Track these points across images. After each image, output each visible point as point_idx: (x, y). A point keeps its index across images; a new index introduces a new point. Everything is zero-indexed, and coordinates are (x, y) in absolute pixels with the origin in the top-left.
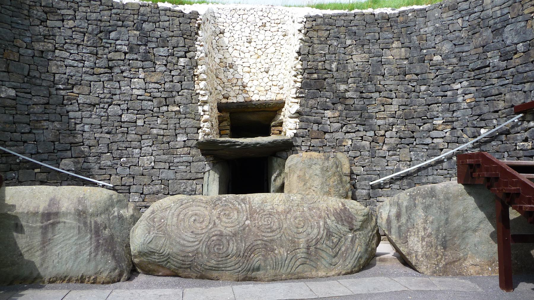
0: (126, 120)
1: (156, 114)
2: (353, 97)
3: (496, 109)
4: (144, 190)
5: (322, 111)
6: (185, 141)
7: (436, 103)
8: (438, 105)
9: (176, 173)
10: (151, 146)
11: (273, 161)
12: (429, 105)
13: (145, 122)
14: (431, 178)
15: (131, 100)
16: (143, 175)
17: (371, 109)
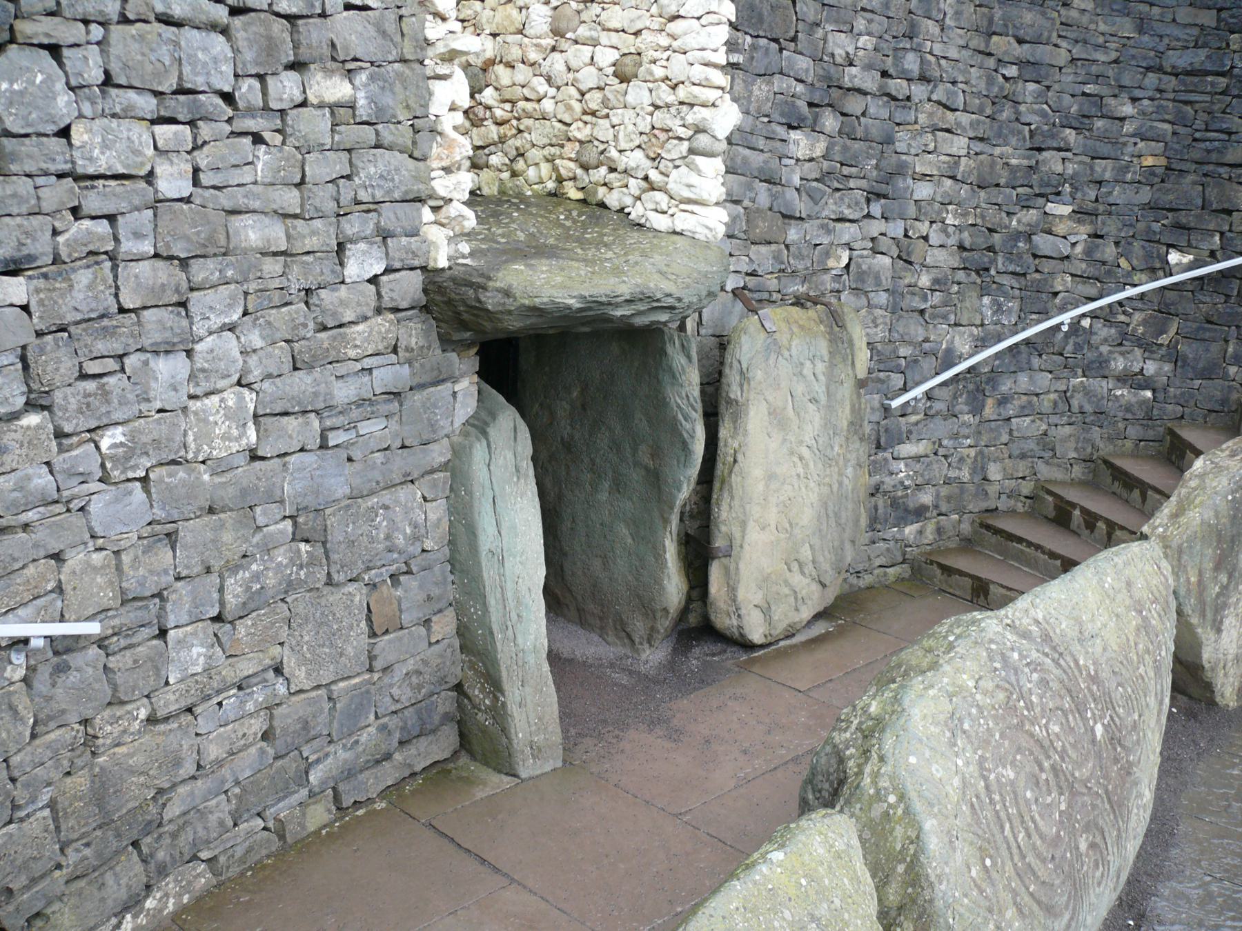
0: (104, 162)
1: (251, 124)
2: (864, 86)
3: (1226, 206)
4: (229, 597)
5: (781, 131)
6: (374, 280)
7: (1059, 149)
8: (1063, 154)
9: (350, 459)
10: (231, 328)
11: (669, 349)
12: (1040, 150)
13: (196, 170)
14: (1023, 378)
15: (124, 20)
16: (211, 511)
17: (903, 140)
